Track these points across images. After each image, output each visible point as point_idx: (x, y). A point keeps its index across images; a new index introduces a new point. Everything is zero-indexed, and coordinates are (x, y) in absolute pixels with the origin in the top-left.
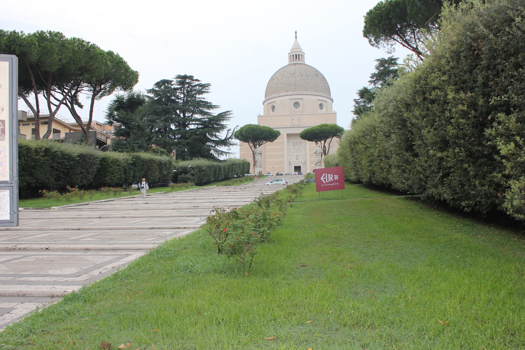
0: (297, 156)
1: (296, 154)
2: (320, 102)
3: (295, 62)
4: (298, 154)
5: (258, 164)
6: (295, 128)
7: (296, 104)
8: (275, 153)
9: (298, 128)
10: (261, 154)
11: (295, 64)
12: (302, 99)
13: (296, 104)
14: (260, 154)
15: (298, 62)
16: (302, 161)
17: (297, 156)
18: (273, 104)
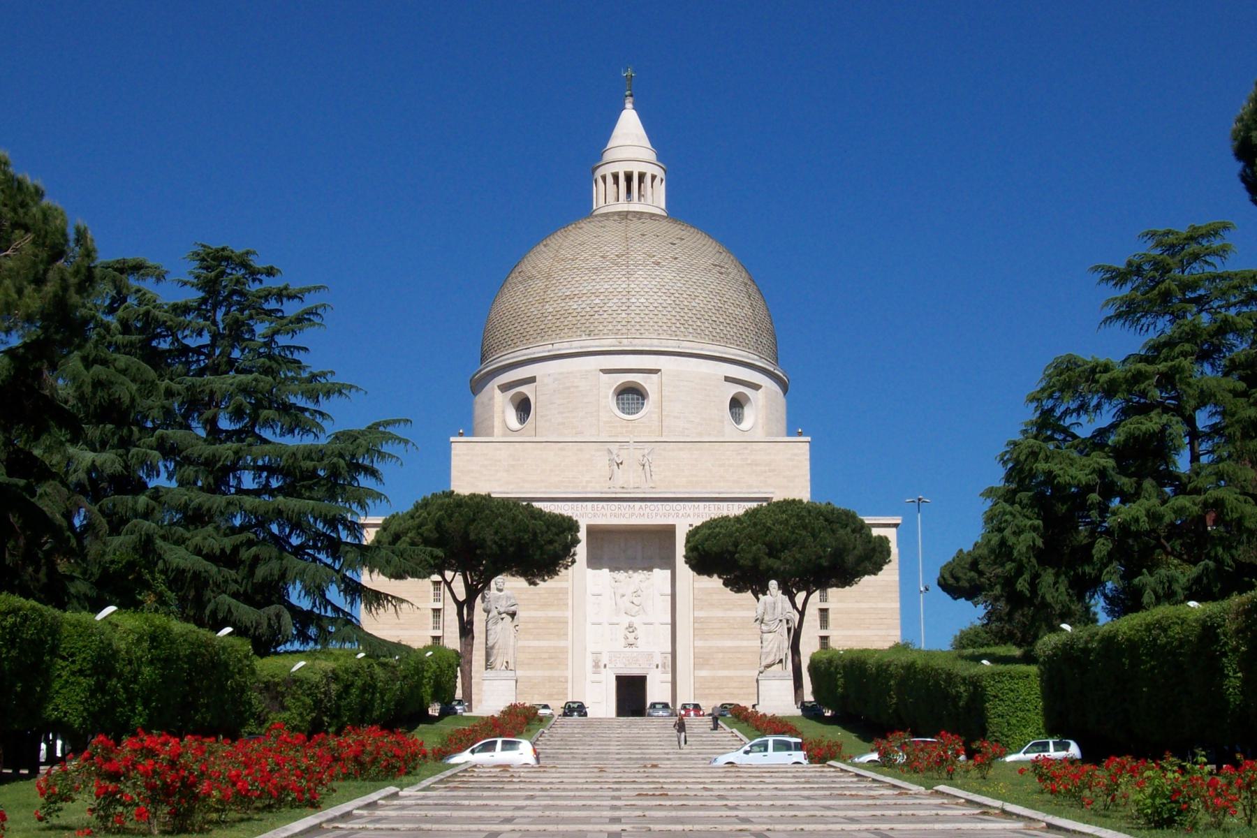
0: (631, 628)
1: (626, 620)
2: (736, 389)
3: (623, 206)
4: (636, 621)
5: (499, 661)
6: (625, 504)
7: (631, 395)
8: (533, 614)
9: (638, 504)
10: (513, 615)
11: (624, 216)
12: (656, 371)
13: (631, 395)
14: (508, 618)
15: (635, 207)
16: (650, 655)
17: (631, 628)
18: (525, 389)
